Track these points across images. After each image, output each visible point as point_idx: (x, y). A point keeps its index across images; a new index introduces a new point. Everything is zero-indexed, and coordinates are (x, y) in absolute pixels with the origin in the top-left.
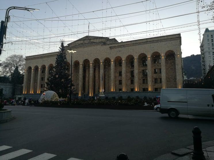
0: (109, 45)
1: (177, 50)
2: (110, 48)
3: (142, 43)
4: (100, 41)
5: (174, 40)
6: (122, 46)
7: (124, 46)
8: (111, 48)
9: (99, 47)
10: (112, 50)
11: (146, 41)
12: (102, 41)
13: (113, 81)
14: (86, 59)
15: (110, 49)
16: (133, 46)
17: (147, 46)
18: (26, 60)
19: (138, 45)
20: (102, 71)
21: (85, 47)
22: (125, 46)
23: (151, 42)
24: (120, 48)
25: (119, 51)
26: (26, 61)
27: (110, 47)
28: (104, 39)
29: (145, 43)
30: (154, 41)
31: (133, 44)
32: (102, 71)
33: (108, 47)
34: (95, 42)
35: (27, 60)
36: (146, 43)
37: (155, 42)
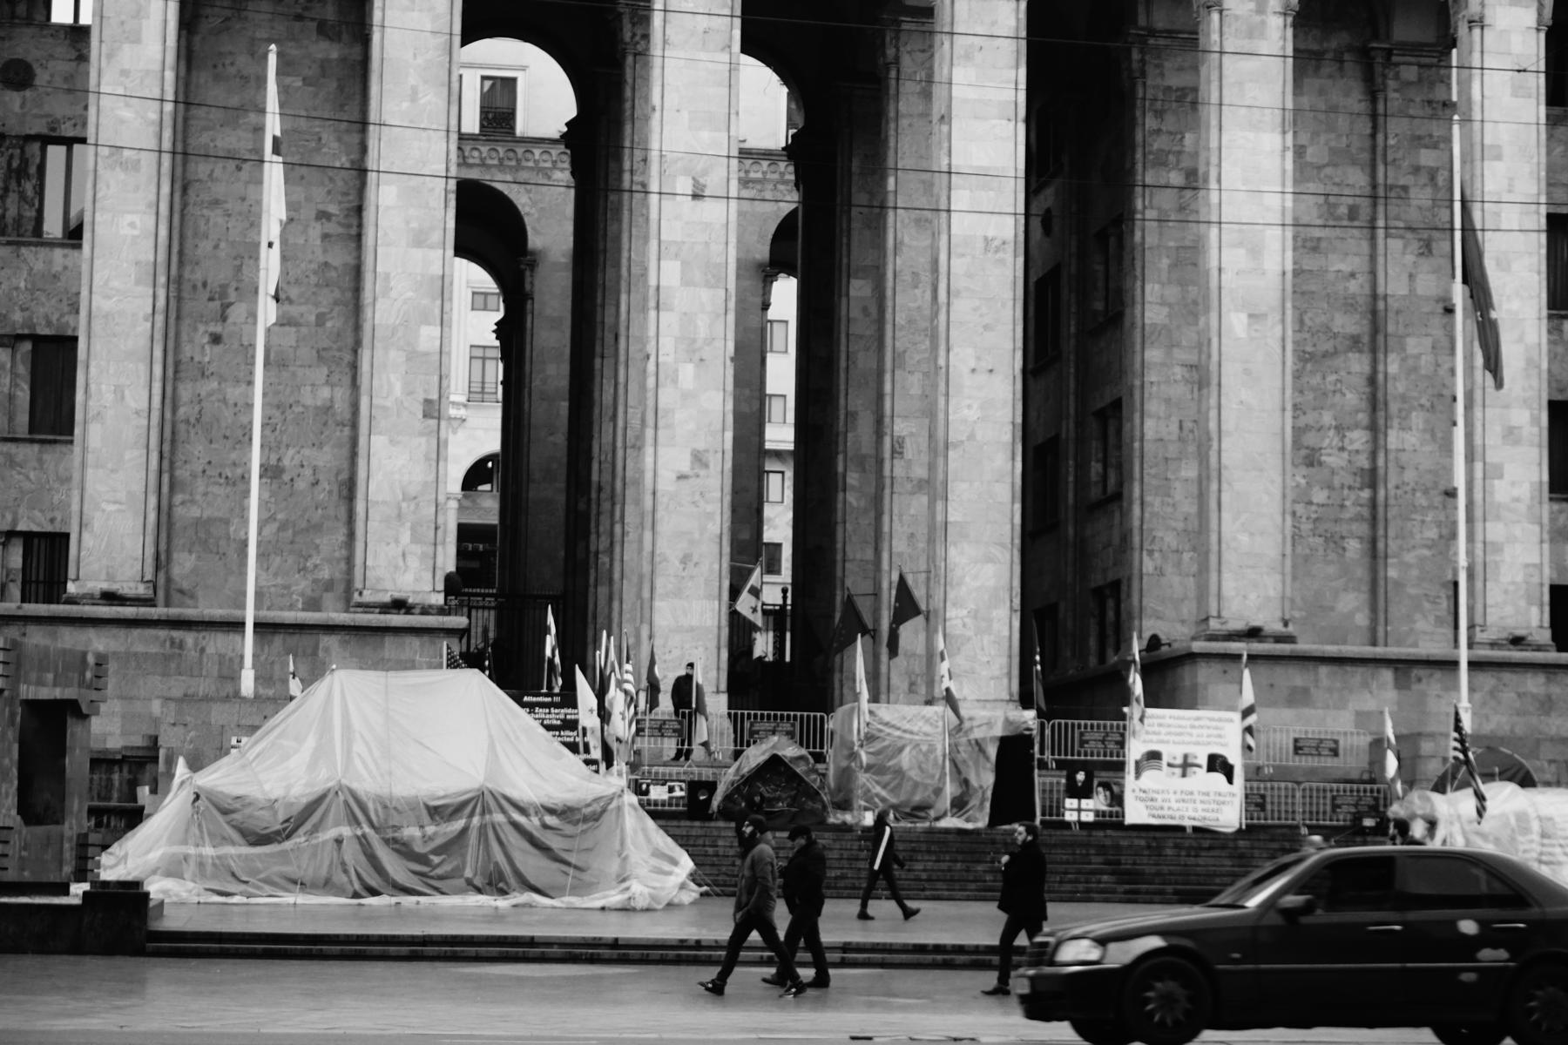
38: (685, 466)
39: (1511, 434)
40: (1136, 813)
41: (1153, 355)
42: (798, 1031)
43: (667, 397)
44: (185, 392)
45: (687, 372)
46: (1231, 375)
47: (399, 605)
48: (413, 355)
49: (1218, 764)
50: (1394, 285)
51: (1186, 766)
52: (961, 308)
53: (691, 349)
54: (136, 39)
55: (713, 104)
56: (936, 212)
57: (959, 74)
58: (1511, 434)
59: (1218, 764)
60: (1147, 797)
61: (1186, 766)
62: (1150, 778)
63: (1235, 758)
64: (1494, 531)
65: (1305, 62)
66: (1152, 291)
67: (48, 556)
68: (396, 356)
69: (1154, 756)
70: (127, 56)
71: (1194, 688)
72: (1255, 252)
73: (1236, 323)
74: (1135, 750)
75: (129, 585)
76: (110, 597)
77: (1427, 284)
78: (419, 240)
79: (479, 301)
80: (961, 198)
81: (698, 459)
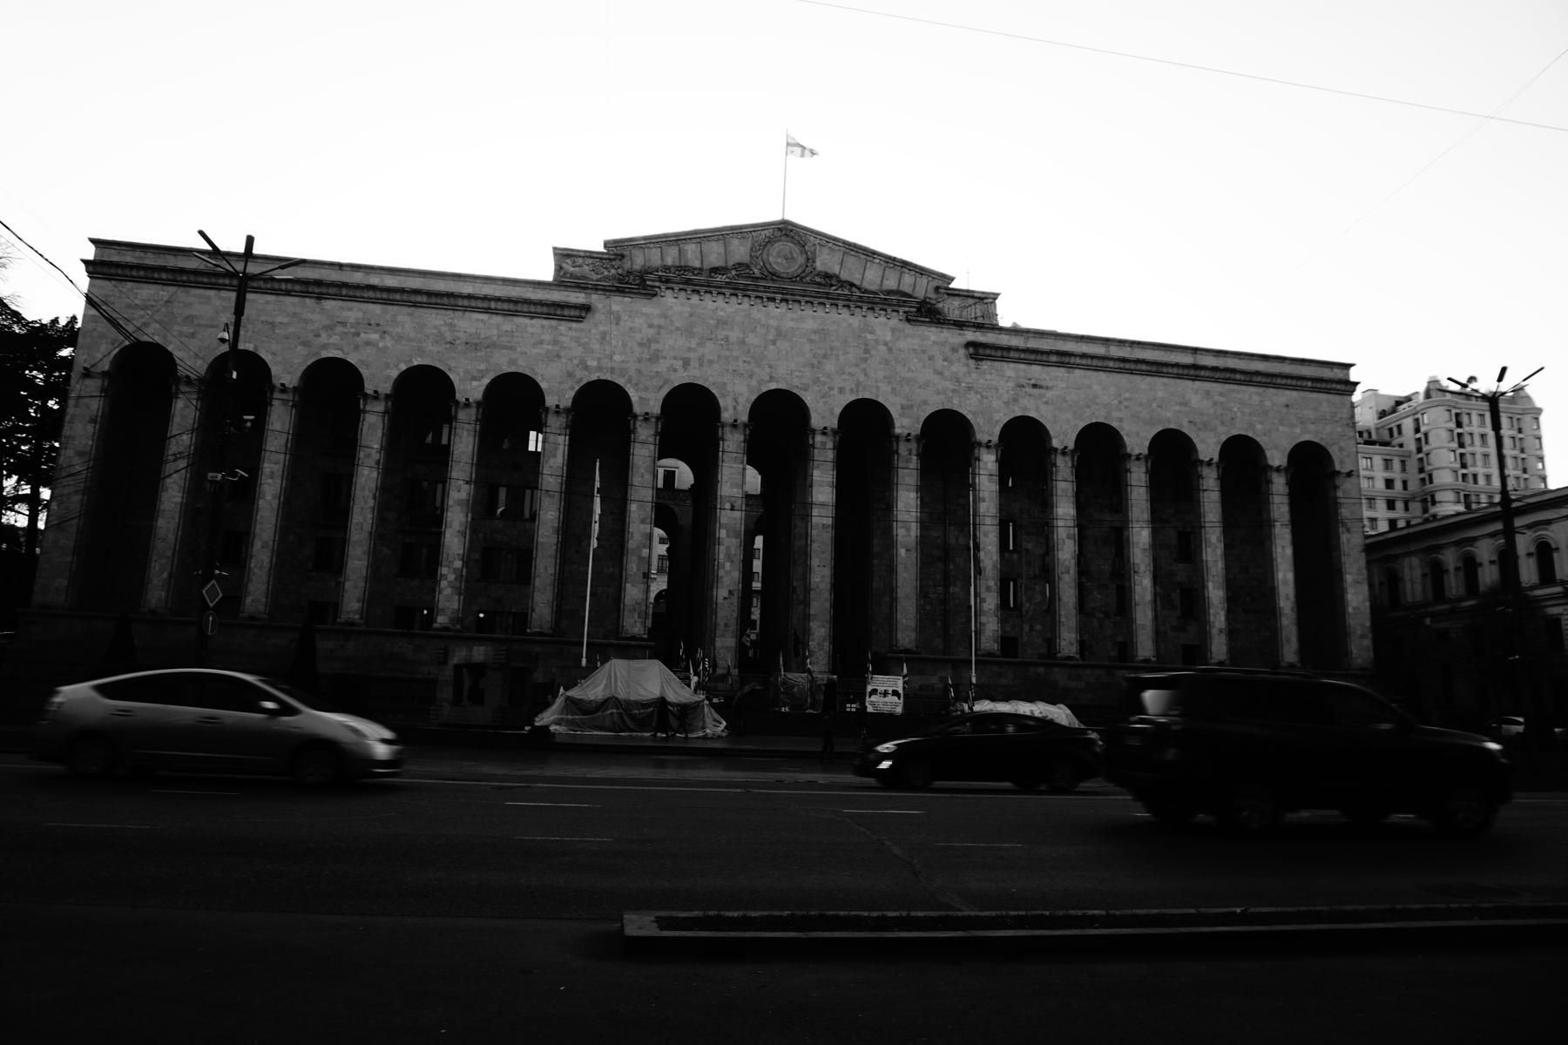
0: (960, 325)
1: (1341, 449)
4: (891, 283)
5: (1328, 391)
6: (1054, 358)
7: (1066, 360)
8: (981, 351)
9: (884, 326)
10: (985, 365)
11: (1187, 359)
12: (906, 288)
13: (992, 583)
14: (783, 386)
15: (972, 357)
17: (1193, 392)
18: (91, 274)
20: (907, 502)
21: (774, 300)
22: (1072, 360)
23: (1218, 375)
24: (1036, 369)
25: (1035, 386)
26: (98, 282)
28: (924, 281)
30: (1234, 371)
31: (1124, 360)
32: (907, 502)
33: (957, 338)
34: (852, 285)
35: (108, 277)
36: (1192, 372)
37: (1238, 376)
38: (726, 594)
39: (988, 589)
40: (870, 709)
41: (876, 562)
42: (857, 923)
43: (721, 573)
45: (728, 565)
46: (900, 568)
47: (633, 638)
48: (640, 558)
49: (895, 693)
50: (953, 542)
51: (885, 694)
52: (815, 546)
53: (729, 557)
54: (555, 456)
55: (739, 479)
56: (807, 516)
57: (816, 473)
58: (988, 589)
59: (895, 693)
60: (872, 704)
61: (885, 694)
62: (874, 698)
63: (901, 691)
64: (984, 619)
65: (924, 472)
66: (875, 541)
67: (522, 619)
68: (634, 558)
69: (874, 692)
70: (552, 462)
72: (908, 530)
73: (902, 552)
74: (869, 688)
75: (546, 628)
76: (540, 634)
77: (962, 541)
78: (643, 522)
79: (662, 541)
80: (815, 512)
81: (731, 592)
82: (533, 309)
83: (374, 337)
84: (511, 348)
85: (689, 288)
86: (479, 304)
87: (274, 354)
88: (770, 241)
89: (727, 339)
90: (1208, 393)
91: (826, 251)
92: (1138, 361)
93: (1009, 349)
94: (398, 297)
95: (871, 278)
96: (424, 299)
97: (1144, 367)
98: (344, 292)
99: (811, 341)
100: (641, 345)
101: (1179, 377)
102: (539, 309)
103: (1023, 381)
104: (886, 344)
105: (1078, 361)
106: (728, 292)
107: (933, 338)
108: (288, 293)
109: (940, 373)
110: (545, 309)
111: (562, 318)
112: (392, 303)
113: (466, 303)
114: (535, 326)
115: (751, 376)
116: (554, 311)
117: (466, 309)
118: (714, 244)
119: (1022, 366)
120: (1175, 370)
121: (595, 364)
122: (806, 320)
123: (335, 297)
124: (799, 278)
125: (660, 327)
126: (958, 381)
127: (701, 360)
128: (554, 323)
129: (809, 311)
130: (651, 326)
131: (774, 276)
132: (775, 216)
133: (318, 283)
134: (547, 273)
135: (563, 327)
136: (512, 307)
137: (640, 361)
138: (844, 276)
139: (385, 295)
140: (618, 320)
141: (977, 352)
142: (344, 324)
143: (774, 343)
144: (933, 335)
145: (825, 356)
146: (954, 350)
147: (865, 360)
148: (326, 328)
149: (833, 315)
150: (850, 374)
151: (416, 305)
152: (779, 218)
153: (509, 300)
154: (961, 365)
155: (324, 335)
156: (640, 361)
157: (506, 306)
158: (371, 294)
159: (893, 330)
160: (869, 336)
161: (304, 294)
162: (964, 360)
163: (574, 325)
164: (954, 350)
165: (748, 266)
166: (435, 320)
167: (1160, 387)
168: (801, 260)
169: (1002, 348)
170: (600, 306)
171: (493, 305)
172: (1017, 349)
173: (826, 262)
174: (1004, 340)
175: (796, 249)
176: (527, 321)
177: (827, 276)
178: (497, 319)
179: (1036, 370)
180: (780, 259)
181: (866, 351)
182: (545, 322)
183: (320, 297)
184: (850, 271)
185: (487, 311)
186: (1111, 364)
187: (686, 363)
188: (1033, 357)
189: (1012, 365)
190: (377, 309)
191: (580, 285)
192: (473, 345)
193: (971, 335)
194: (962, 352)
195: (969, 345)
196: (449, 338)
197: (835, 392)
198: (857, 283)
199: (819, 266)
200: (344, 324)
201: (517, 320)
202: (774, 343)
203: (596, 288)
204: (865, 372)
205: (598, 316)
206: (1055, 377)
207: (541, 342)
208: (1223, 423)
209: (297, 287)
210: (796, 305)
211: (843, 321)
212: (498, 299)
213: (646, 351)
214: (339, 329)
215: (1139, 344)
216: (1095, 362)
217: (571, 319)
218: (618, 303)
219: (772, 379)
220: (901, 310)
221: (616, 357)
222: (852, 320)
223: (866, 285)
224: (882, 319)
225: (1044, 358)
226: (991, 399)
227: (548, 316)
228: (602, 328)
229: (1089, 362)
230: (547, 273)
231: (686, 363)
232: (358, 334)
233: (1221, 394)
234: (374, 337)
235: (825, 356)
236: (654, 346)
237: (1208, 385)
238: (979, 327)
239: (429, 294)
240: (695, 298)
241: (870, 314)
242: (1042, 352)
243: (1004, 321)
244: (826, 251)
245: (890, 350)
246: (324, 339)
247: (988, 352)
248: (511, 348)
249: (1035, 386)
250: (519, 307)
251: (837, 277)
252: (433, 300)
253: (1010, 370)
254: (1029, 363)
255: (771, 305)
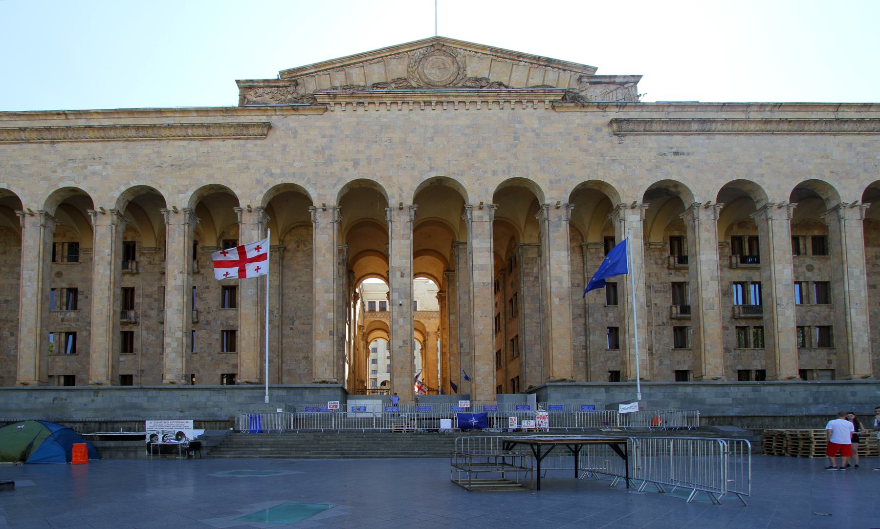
0: (602, 106)
2: (615, 126)
3: (816, 122)
6: (695, 127)
7: (707, 126)
8: (624, 126)
9: (532, 116)
10: (628, 140)
16: (760, 133)
19: (789, 133)
22: (713, 127)
23: (863, 127)
25: (676, 153)
27: (618, 121)
29: (828, 127)
31: (766, 121)
33: (600, 118)
34: (500, 84)
36: (835, 127)
44: (284, 341)
71: (547, 395)
82: (222, 131)
83: (98, 168)
84: (208, 166)
85: (355, 101)
86: (178, 132)
87: (23, 189)
88: (425, 57)
89: (390, 140)
90: (850, 145)
91: (476, 60)
92: (781, 121)
93: (651, 121)
94: (112, 133)
95: (518, 78)
96: (133, 133)
97: (785, 126)
98: (70, 134)
99: (464, 135)
100: (316, 152)
101: (822, 133)
102: (228, 131)
103: (665, 151)
104: (533, 130)
105: (719, 126)
106: (388, 100)
107: (577, 121)
108: (28, 141)
109: (585, 151)
110: (232, 131)
111: (248, 137)
112: (109, 139)
113: (167, 132)
114: (229, 146)
115: (413, 168)
116: (241, 131)
117: (170, 138)
118: (375, 66)
119: (664, 138)
120: (817, 127)
121: (278, 171)
122: (459, 118)
123: (65, 139)
124: (452, 84)
125: (331, 136)
126: (602, 155)
127: (369, 160)
128: (241, 142)
129: (462, 110)
130: (324, 136)
131: (430, 85)
132: (427, 33)
133: (49, 129)
134: (232, 99)
135: (250, 144)
136: (205, 131)
137: (316, 165)
138: (492, 79)
139: (102, 134)
140: (295, 134)
141: (620, 128)
142: (73, 160)
143: (432, 139)
144: (575, 117)
145: (478, 146)
146: (598, 130)
147: (515, 146)
148: (63, 164)
149: (485, 110)
150: (501, 159)
151: (128, 139)
152: (433, 35)
153: (202, 126)
154: (605, 141)
155: (59, 171)
156: (316, 165)
157: (200, 132)
158: (91, 134)
159: (540, 119)
160: (517, 126)
161: (40, 140)
162: (609, 138)
163: (259, 142)
164: (598, 130)
165: (405, 79)
166: (145, 149)
167: (802, 144)
168: (453, 69)
169: (645, 122)
170: (279, 124)
171: (190, 132)
172: (660, 121)
173: (476, 68)
174: (646, 115)
175: (448, 60)
176: (219, 143)
177: (477, 80)
178: (195, 144)
179: (677, 141)
180: (435, 71)
181: (516, 139)
182: (235, 142)
183: (53, 142)
184: (499, 73)
185: (185, 137)
186: (752, 127)
187: (356, 163)
188: (674, 128)
189: (654, 137)
190: (98, 146)
191: (263, 108)
192: (178, 167)
193: (613, 114)
194: (606, 130)
195: (611, 122)
196: (158, 163)
197: (489, 174)
198: (505, 83)
199: (470, 74)
200: (73, 160)
201: (211, 143)
202: (432, 139)
203: (274, 109)
204: (516, 158)
205: (278, 133)
206: (698, 146)
207: (233, 158)
208: (866, 170)
209: (34, 135)
210: (450, 106)
211: (492, 115)
212: (193, 126)
213: (320, 158)
214: (70, 165)
215: (780, 105)
216: (737, 126)
217: (256, 137)
218: (294, 120)
219: (432, 169)
220: (547, 99)
221: (295, 165)
222: (501, 114)
223: (511, 85)
224: (530, 110)
225: (686, 127)
226: (629, 175)
227: (237, 137)
228: (282, 142)
229: (730, 127)
230: (232, 99)
231: (356, 163)
232: (85, 167)
233: (864, 145)
234: (98, 168)
235: (478, 146)
236: (327, 152)
237: (849, 138)
238: (621, 106)
239: (137, 128)
240: (361, 110)
241: (518, 106)
242: (684, 122)
243: (642, 100)
244: (476, 60)
245: (538, 135)
246: (59, 173)
247: (631, 127)
248: (208, 166)
249: (676, 153)
250: (212, 131)
251: (487, 80)
252: (141, 133)
253: (651, 141)
254: (669, 133)
255: (428, 109)
